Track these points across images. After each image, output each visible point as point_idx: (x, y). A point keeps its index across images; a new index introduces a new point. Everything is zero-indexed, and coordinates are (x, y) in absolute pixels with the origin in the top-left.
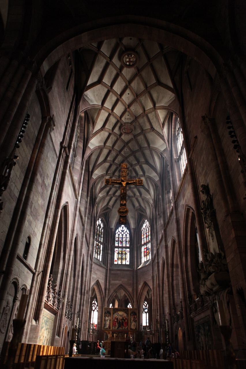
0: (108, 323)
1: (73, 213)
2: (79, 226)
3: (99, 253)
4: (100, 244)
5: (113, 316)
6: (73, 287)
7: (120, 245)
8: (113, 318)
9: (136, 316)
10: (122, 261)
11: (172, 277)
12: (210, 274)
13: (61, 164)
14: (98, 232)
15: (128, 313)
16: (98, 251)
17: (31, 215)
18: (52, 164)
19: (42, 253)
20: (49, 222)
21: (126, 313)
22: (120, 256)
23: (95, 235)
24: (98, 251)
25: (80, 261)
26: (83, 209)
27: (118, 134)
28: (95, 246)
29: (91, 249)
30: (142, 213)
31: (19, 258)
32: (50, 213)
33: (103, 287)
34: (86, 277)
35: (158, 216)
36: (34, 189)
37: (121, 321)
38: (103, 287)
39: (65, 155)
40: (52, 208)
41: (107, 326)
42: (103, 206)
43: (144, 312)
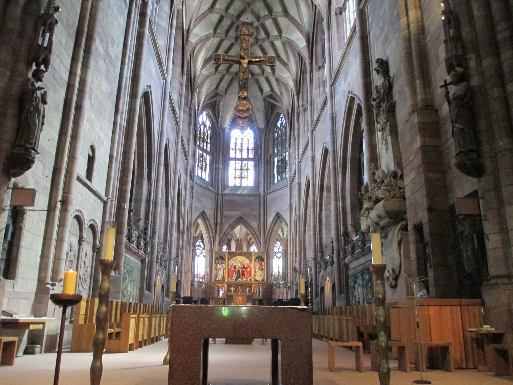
0: (221, 273)
1: (160, 103)
2: (170, 125)
3: (204, 169)
4: (205, 154)
5: (228, 263)
6: (165, 222)
7: (239, 156)
8: (228, 266)
9: (263, 263)
10: (241, 180)
11: (321, 205)
12: (377, 201)
13: (134, 18)
14: (202, 135)
15: (251, 259)
16: (202, 165)
18: (119, 18)
19: (115, 171)
20: (122, 120)
21: (249, 259)
22: (238, 173)
23: (198, 139)
24: (202, 165)
25: (175, 182)
26: (175, 97)
28: (197, 157)
29: (190, 161)
30: (275, 103)
31: (79, 179)
32: (123, 106)
34: (185, 206)
35: (301, 109)
37: (240, 270)
40: (124, 97)
41: (220, 278)
43: (275, 257)
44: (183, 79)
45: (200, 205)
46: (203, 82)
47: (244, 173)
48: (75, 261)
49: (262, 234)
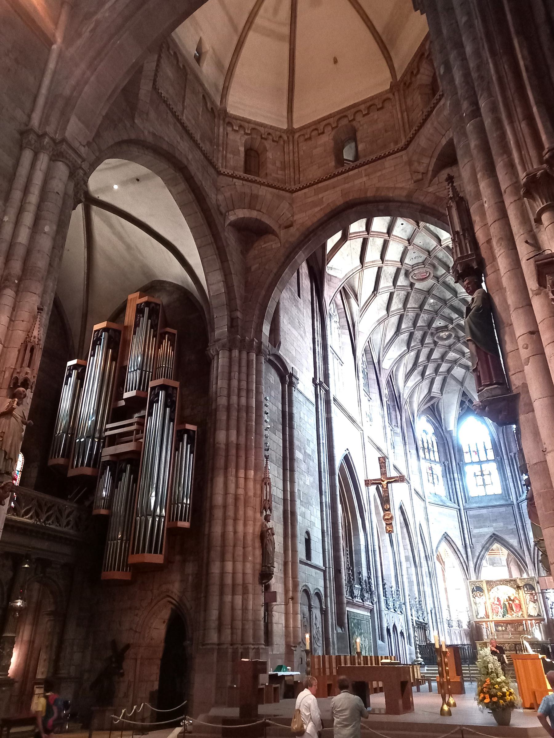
7: (476, 459)
9: (533, 592)
18: (310, 421)
19: (328, 543)
20: (327, 499)
31: (301, 562)
36: (296, 469)
37: (507, 603)
38: (459, 544)
39: (323, 392)
40: (325, 478)
41: (482, 614)
46: (411, 396)
49: (526, 553)
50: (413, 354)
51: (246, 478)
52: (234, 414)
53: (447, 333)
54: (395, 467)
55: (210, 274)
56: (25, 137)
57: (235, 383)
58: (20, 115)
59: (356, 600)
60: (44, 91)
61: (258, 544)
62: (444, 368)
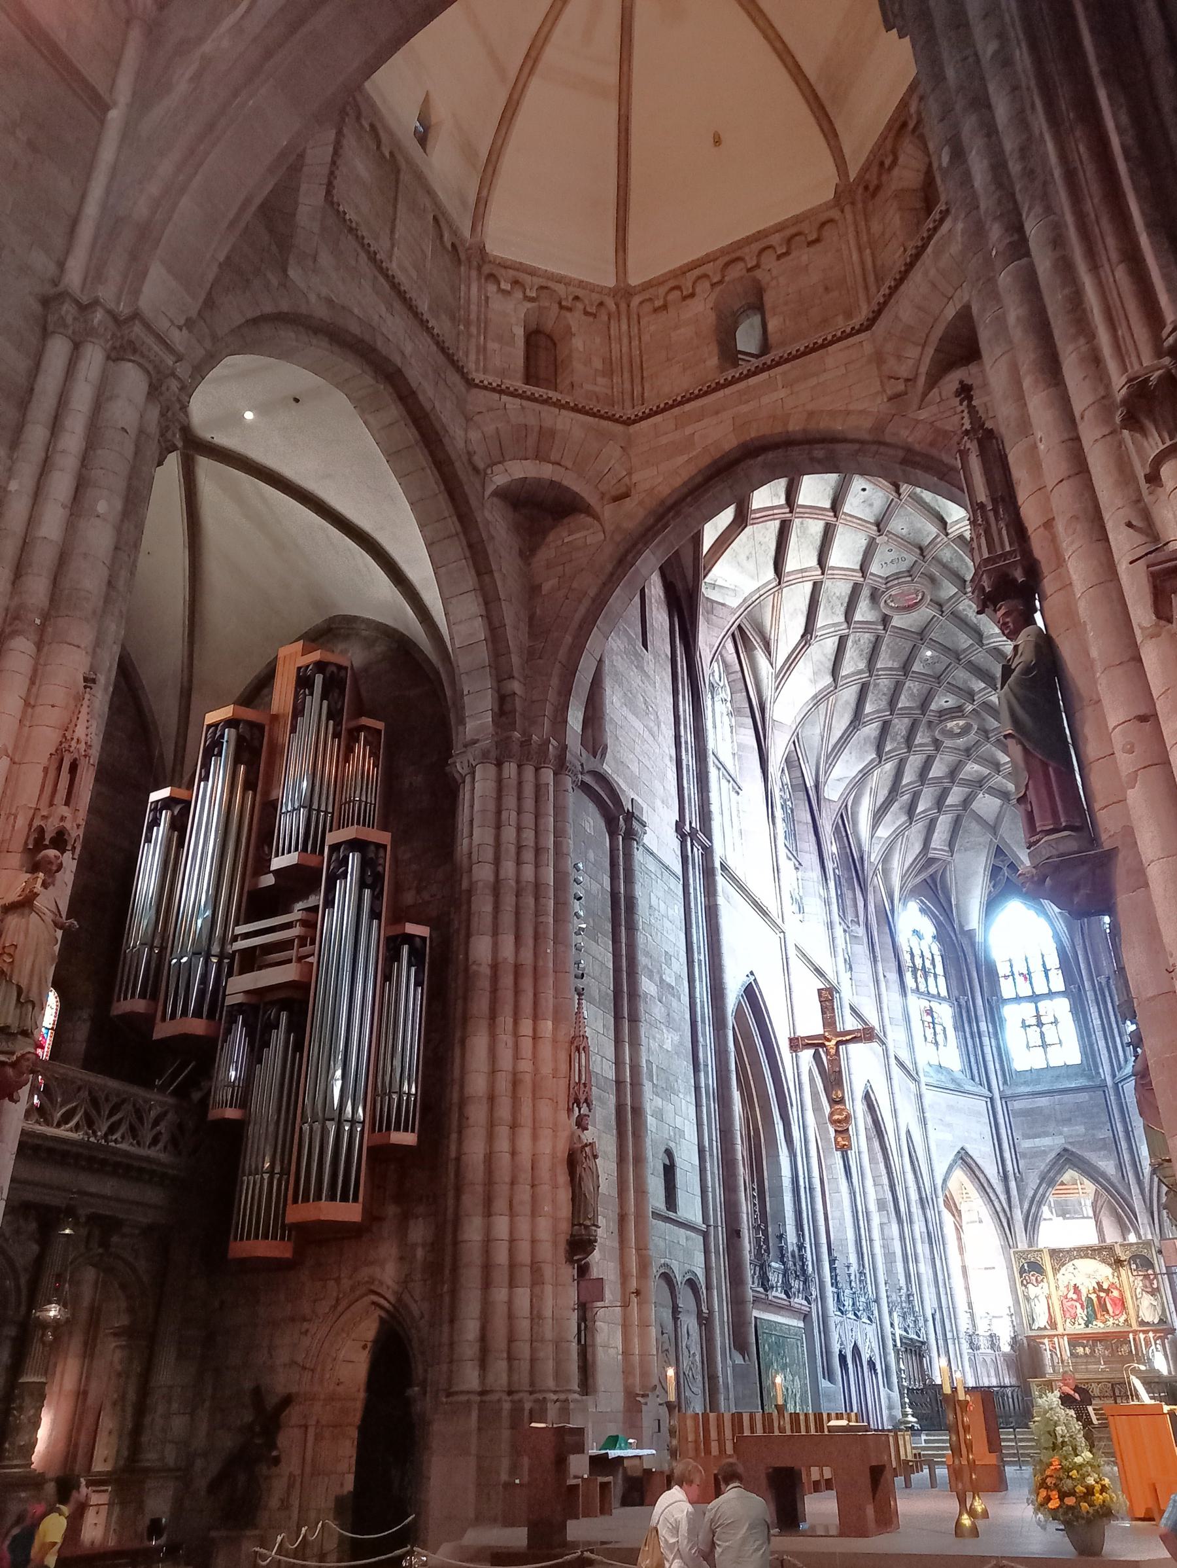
7: (1025, 990)
9: (1150, 1272)
10: (1045, 1052)
17: (657, 1095)
18: (670, 912)
19: (712, 1173)
20: (709, 1079)
27: (874, 619)
31: (656, 1215)
33: (991, 1171)
36: (643, 1016)
37: (1093, 1296)
38: (991, 1171)
39: (698, 852)
40: (704, 1035)
41: (1042, 1321)
42: (910, 860)
44: (828, 889)
45: (948, 1137)
46: (886, 858)
47: (1050, 1033)
48: (672, 1350)
50: (889, 767)
51: (535, 1038)
52: (508, 901)
53: (961, 723)
54: (852, 1008)
55: (454, 601)
56: (52, 310)
57: (509, 834)
58: (42, 262)
59: (774, 1293)
60: (92, 209)
61: (563, 1178)
62: (955, 796)
